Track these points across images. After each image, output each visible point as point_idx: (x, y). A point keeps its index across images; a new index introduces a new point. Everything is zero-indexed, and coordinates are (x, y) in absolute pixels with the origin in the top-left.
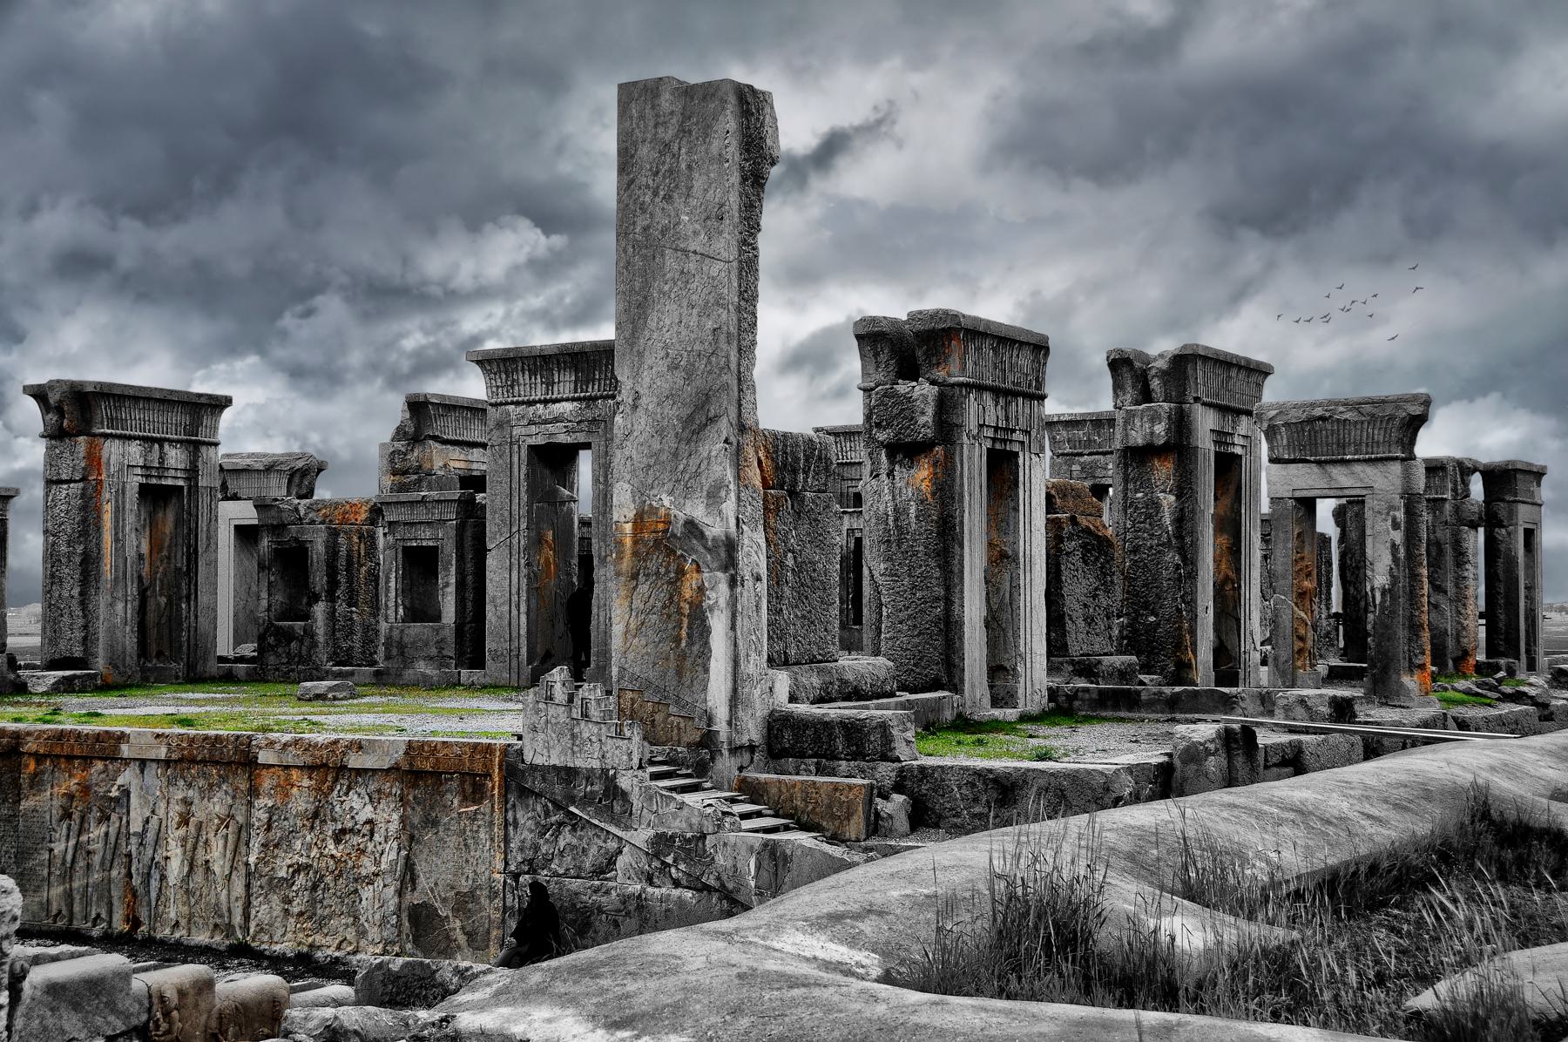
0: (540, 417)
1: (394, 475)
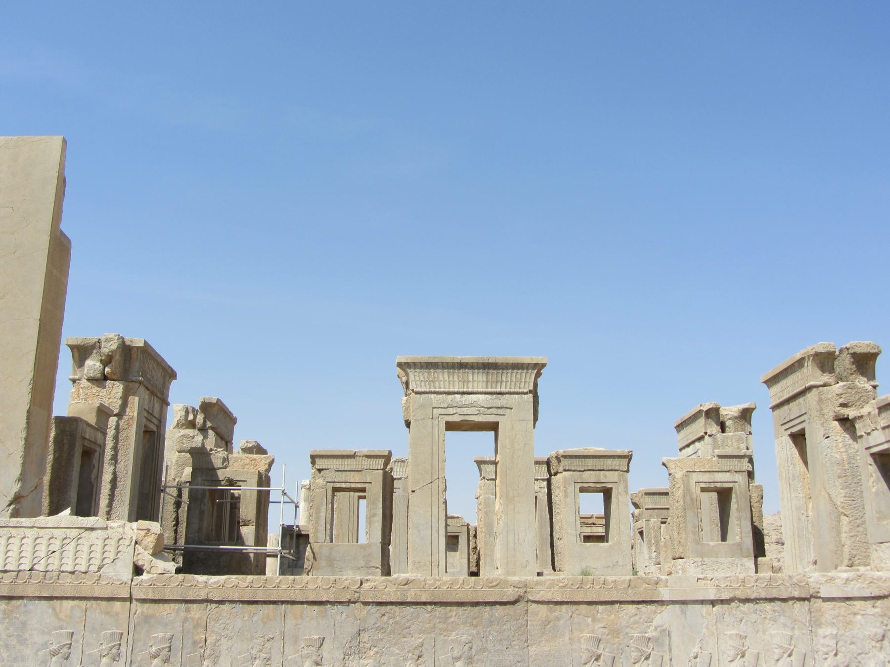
0: (457, 402)
1: (179, 452)
